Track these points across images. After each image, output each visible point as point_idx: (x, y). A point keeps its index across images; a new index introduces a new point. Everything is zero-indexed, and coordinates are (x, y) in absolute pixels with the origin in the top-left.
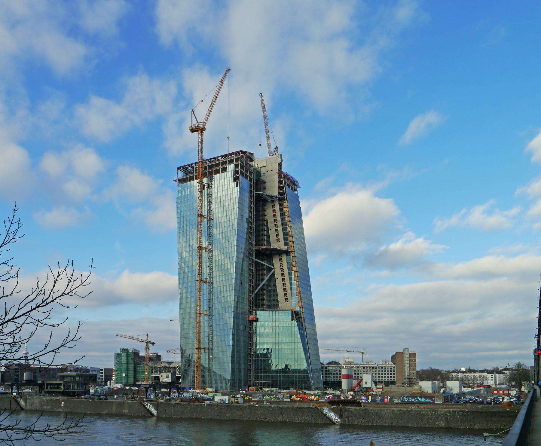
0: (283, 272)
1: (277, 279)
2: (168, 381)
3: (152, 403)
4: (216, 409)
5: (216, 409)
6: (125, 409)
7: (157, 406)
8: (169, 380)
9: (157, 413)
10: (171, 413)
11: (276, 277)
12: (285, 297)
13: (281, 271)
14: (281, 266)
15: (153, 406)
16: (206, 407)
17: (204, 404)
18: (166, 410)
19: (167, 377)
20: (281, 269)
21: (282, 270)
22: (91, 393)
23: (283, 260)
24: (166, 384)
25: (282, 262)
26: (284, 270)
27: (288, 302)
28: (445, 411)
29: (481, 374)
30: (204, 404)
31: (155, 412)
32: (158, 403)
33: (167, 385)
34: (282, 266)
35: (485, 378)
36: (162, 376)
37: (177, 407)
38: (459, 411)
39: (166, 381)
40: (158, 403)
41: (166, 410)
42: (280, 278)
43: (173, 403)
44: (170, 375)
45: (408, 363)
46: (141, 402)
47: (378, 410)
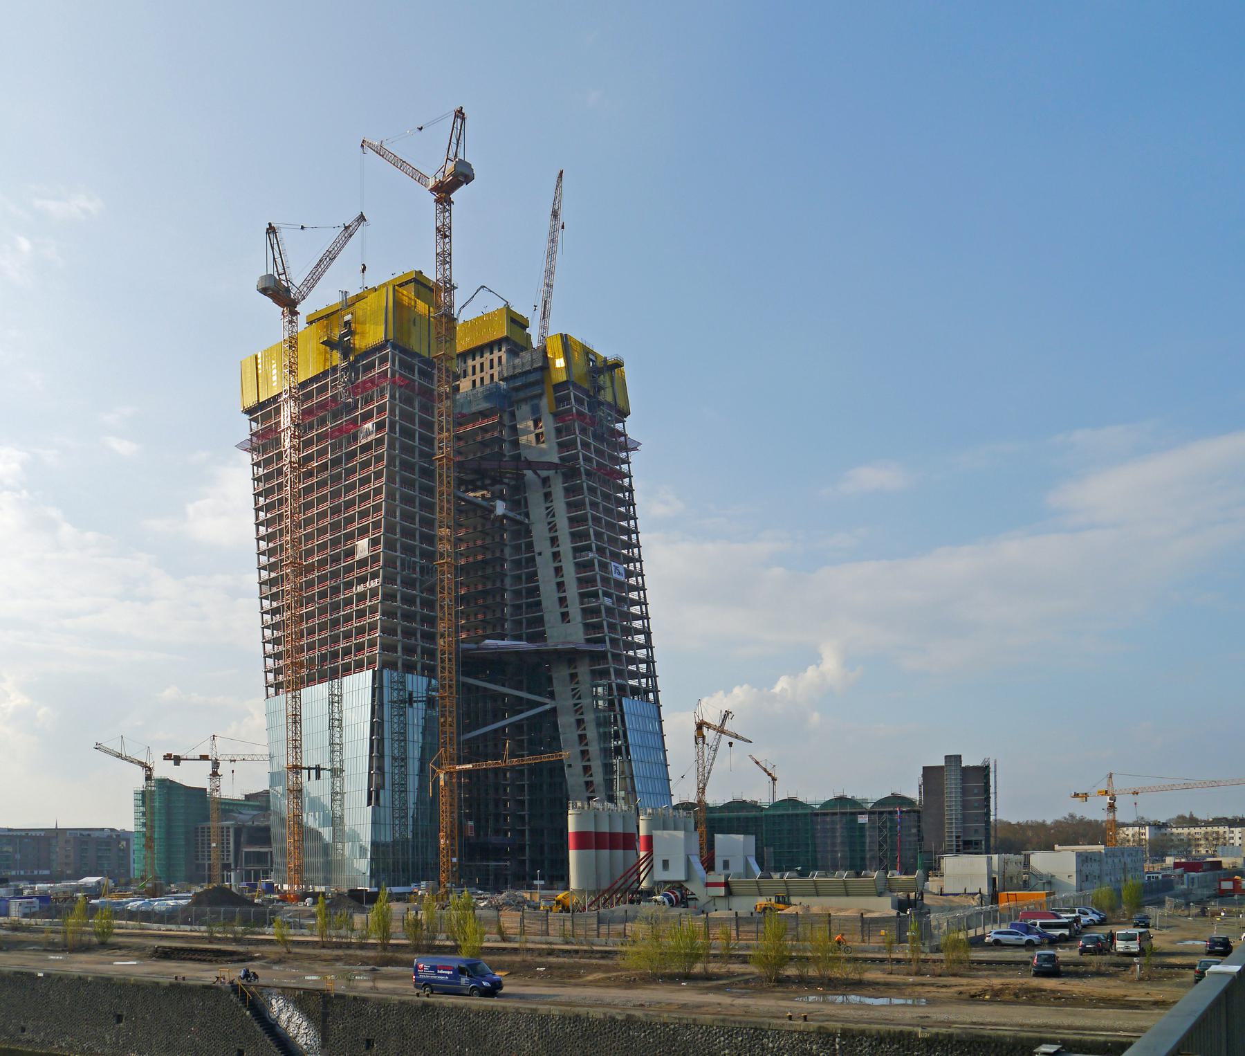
0: (556, 531)
1: (540, 554)
11: (537, 549)
12: (561, 607)
13: (550, 530)
14: (548, 514)
20: (549, 523)
21: (553, 527)
23: (554, 496)
25: (552, 501)
26: (558, 527)
27: (569, 622)
28: (801, 1033)
29: (1209, 829)
34: (551, 513)
35: (1221, 840)
38: (878, 1032)
42: (548, 551)
45: (959, 798)
47: (477, 1014)
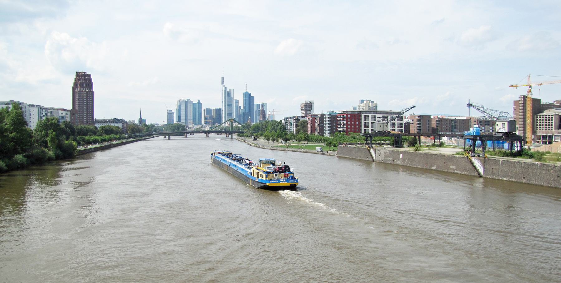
2: (504, 132)
3: (479, 159)
4: (552, 171)
5: (552, 171)
6: (453, 165)
7: (484, 162)
8: (506, 130)
9: (484, 171)
10: (499, 174)
15: (481, 162)
16: (539, 168)
17: (538, 164)
18: (493, 168)
19: (503, 125)
22: (445, 145)
24: (501, 135)
30: (538, 164)
31: (481, 170)
32: (485, 160)
33: (502, 136)
36: (497, 125)
37: (505, 165)
39: (502, 132)
40: (485, 159)
41: (493, 168)
43: (501, 160)
44: (506, 124)
46: (468, 157)
